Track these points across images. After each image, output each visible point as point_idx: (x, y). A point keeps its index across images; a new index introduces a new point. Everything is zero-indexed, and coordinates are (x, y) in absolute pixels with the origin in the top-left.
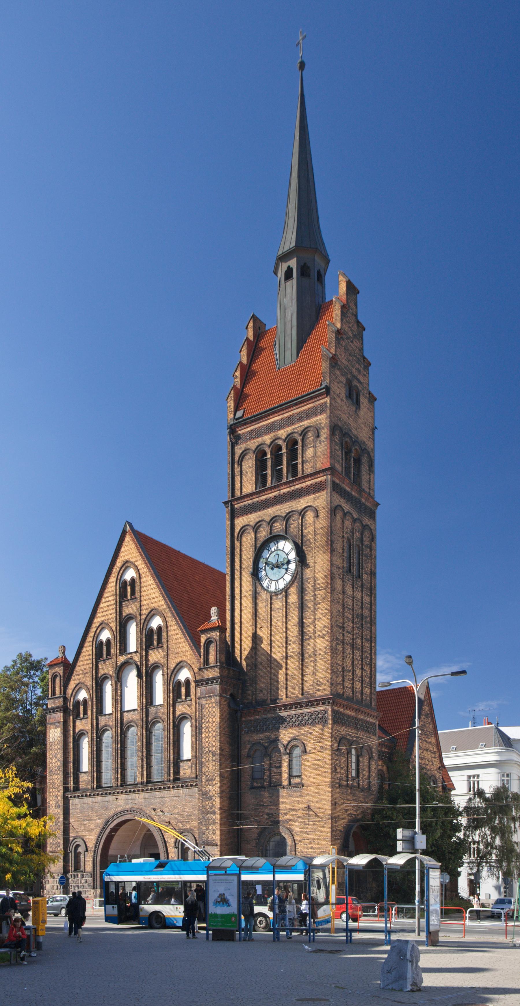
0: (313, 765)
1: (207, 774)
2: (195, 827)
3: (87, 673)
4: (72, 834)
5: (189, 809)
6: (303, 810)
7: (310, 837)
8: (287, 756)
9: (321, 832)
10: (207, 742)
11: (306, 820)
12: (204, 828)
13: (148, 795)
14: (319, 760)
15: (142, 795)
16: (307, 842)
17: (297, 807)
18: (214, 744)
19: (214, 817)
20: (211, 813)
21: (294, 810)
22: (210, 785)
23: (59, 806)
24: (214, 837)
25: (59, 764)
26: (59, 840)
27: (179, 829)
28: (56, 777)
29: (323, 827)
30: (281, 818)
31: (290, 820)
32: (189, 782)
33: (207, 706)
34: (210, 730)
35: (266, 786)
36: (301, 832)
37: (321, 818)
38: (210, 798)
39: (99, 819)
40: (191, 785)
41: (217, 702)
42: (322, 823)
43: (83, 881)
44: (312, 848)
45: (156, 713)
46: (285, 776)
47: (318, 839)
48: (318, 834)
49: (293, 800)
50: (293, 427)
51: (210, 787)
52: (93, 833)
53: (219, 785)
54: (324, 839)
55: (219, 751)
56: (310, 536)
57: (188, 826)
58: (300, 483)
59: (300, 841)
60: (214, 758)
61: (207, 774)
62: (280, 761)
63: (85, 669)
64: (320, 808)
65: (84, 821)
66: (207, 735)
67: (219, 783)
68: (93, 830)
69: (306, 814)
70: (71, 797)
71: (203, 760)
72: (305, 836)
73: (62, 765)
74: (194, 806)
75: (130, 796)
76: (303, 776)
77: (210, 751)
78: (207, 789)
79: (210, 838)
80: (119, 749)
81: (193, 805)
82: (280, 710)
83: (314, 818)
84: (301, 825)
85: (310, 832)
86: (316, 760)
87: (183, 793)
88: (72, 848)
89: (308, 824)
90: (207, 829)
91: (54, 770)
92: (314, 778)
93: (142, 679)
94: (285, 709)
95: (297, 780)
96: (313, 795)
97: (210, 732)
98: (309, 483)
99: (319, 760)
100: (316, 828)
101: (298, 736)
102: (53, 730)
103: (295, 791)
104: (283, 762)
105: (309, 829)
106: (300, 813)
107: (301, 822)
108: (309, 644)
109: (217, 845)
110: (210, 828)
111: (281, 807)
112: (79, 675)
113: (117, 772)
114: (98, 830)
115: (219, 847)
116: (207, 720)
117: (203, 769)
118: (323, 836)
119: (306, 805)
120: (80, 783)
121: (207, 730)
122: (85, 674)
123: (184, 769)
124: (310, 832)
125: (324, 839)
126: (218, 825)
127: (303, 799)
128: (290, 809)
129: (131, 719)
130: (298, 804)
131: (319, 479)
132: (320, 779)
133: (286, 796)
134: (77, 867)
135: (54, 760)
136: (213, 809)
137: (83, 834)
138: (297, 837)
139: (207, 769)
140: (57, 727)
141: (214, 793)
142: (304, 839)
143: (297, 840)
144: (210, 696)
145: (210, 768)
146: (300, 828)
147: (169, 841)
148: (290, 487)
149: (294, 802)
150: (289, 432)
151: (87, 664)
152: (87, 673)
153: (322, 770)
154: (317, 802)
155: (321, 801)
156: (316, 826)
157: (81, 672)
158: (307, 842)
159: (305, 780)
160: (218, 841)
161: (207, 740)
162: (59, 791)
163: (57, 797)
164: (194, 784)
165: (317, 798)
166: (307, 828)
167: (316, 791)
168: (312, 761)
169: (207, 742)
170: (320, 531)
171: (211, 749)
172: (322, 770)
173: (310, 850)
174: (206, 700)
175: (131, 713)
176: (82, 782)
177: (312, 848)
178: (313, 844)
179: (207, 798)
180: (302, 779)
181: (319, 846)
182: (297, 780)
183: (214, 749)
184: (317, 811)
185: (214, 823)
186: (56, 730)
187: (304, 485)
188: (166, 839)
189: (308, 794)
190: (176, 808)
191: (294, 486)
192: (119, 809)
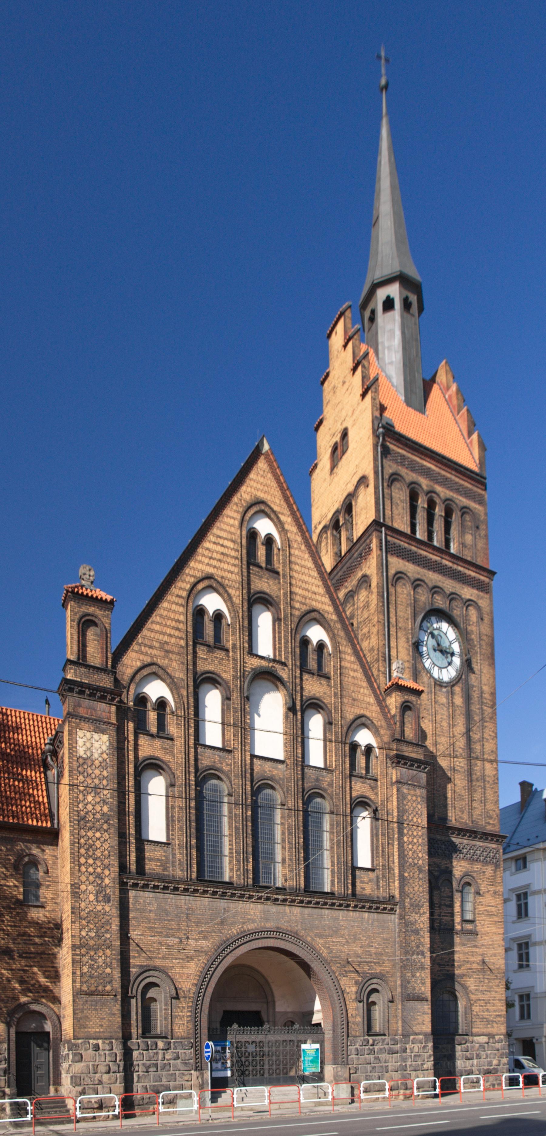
0: (486, 911)
1: (411, 896)
2: (387, 972)
4: (136, 961)
5: (378, 944)
6: (478, 964)
7: (486, 997)
8: (460, 894)
9: (496, 992)
10: (410, 850)
11: (481, 977)
12: (409, 974)
13: (307, 911)
14: (493, 906)
15: (297, 911)
16: (482, 1003)
17: (472, 959)
18: (420, 855)
19: (423, 960)
20: (418, 954)
21: (468, 962)
22: (416, 913)
23: (107, 899)
24: (423, 988)
25: (105, 809)
26: (108, 970)
27: (364, 973)
28: (98, 835)
29: (498, 986)
30: (457, 972)
31: (464, 975)
32: (383, 903)
33: (409, 797)
34: (415, 833)
35: (437, 928)
36: (476, 990)
37: (496, 976)
38: (417, 932)
39: (205, 938)
40: (385, 909)
41: (423, 798)
42: (497, 982)
43: (168, 1056)
44: (488, 1010)
45: (317, 780)
46: (457, 919)
47: (493, 1000)
48: (493, 994)
49: (467, 950)
50: (455, 496)
51: (417, 917)
52: (192, 964)
53: (428, 915)
54: (500, 1000)
55: (427, 868)
56: (473, 636)
57: (378, 970)
58: (464, 567)
59: (475, 1002)
60: (421, 876)
61: (411, 896)
62: (451, 898)
63: (166, 643)
64: (494, 963)
65: (167, 936)
66: (410, 839)
67: (428, 912)
68: (189, 958)
69: (481, 969)
70: (135, 885)
71: (406, 875)
72: (480, 996)
73: (114, 814)
74: (387, 940)
75: (274, 909)
76: (477, 923)
77: (415, 864)
78: (412, 919)
79: (417, 989)
80: (250, 819)
81: (384, 940)
82: (453, 833)
83: (489, 975)
84: (476, 981)
85: (486, 991)
86: (489, 906)
87: (368, 919)
88: (136, 990)
89: (483, 982)
90: (413, 976)
91: (90, 817)
92: (488, 927)
93: (296, 715)
94: (458, 834)
95: (469, 926)
96: (488, 946)
97: (415, 837)
98: (473, 574)
99: (493, 906)
100: (492, 987)
101: (471, 872)
102: (88, 735)
103: (469, 940)
104: (455, 900)
105: (484, 988)
106: (475, 966)
107: (476, 978)
108: (476, 764)
109: (427, 1001)
110: (418, 974)
111: (456, 957)
112: (151, 647)
113: (246, 860)
114: (203, 959)
115: (429, 1003)
116: (410, 818)
117: (406, 888)
118: (498, 996)
119: (480, 958)
120: (147, 862)
121: (410, 833)
122: (167, 651)
123: (362, 882)
124: (486, 991)
125: (500, 1000)
126: (428, 971)
127: (477, 950)
128: (464, 961)
129: (268, 774)
130: (473, 956)
131: (482, 578)
132: (494, 930)
133: (460, 944)
134: (147, 1029)
135: (90, 798)
136: (421, 948)
137: (167, 963)
138: (473, 997)
139: (411, 890)
140: (98, 730)
141: (422, 926)
142: (480, 1000)
143: (472, 1000)
144: (415, 785)
145: (416, 888)
146: (475, 986)
147: (348, 990)
148: (453, 563)
149: (467, 953)
150: (448, 497)
151: (170, 635)
153: (496, 919)
154: (491, 956)
155: (495, 955)
156: (491, 984)
157: (157, 645)
158: (482, 1003)
159: (479, 928)
160: (429, 995)
161: (410, 846)
162: (106, 867)
163: (102, 879)
164: (389, 907)
165: (491, 951)
166: (483, 986)
167: (490, 943)
168: (486, 906)
169: (410, 850)
170: (485, 638)
171: (416, 862)
172: (496, 919)
173: (486, 1013)
174: (409, 789)
175: (269, 763)
176: (151, 860)
177: (488, 1010)
178: (489, 1007)
179: (412, 931)
180: (476, 926)
181: (495, 1008)
182: (469, 926)
183: (420, 862)
184: (492, 967)
185: (422, 968)
186: (96, 736)
187: (468, 572)
188: (342, 987)
189: (483, 945)
190: (359, 939)
191: (458, 565)
192: (251, 927)
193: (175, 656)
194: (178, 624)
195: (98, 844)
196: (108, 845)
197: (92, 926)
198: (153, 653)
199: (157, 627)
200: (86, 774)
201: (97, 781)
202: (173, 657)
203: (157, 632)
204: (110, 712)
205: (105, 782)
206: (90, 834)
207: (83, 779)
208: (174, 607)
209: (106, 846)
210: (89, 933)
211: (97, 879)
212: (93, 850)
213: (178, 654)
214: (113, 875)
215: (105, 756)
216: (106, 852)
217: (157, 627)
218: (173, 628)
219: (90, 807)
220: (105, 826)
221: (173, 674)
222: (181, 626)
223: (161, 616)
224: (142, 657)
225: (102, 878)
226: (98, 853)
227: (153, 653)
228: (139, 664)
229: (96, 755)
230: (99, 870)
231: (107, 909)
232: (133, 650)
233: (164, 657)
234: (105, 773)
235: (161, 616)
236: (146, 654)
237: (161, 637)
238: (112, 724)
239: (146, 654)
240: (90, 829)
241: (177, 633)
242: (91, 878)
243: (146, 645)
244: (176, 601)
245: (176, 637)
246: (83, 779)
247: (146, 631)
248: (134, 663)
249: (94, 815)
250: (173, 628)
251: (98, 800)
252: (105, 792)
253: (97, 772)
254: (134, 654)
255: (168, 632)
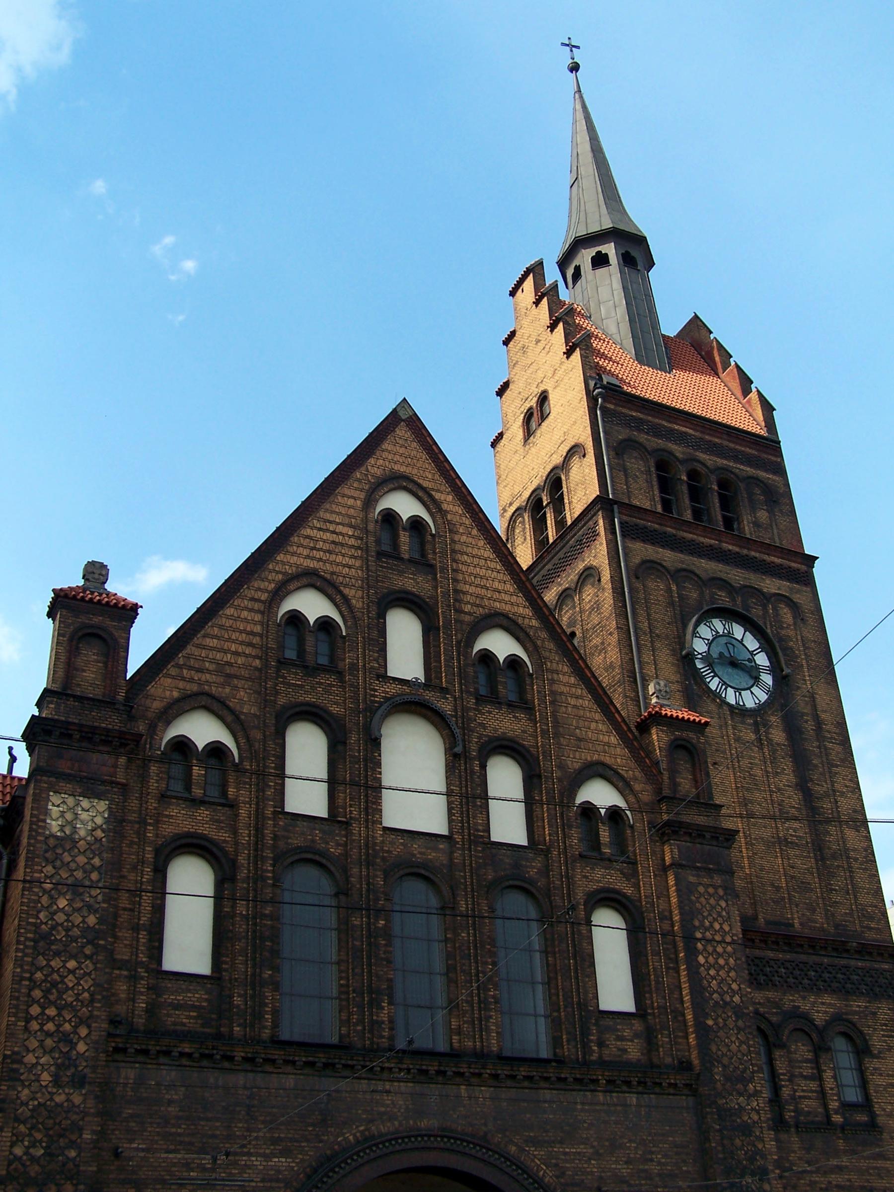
3: (236, 677)
23: (79, 1082)
25: (92, 920)
28: (72, 964)
91: (60, 935)
102: (71, 801)
112: (199, 670)
122: (229, 676)
135: (62, 903)
140: (91, 793)
151: (236, 653)
152: (236, 677)
157: (212, 667)
162: (82, 1022)
186: (85, 803)
193: (243, 682)
194: (251, 637)
195: (70, 981)
196: (91, 982)
197: (38, 1136)
198: (203, 678)
199: (214, 643)
200: (58, 863)
201: (79, 874)
202: (241, 683)
203: (212, 649)
204: (115, 766)
205: (94, 876)
206: (56, 963)
207: (54, 871)
208: (245, 614)
209: (86, 984)
210: (32, 1150)
211: (61, 1045)
212: (58, 992)
213: (249, 679)
214: (95, 1036)
215: (99, 834)
216: (86, 995)
217: (210, 642)
218: (242, 643)
219: (60, 918)
220: (88, 951)
221: (238, 708)
222: (256, 640)
223: (221, 627)
224: (181, 684)
225: (71, 1042)
226: (69, 997)
227: (203, 678)
228: (176, 694)
229: (82, 833)
230: (67, 1027)
231: (77, 1099)
232: (168, 676)
233: (223, 685)
234: (97, 861)
235: (221, 627)
236: (191, 680)
237: (219, 656)
238: (118, 783)
239: (191, 680)
240: (57, 954)
241: (248, 651)
242: (49, 1042)
243: (191, 668)
244: (250, 606)
245: (247, 656)
246: (54, 871)
247: (193, 648)
248: (168, 693)
249: (67, 930)
250: (242, 643)
251: (78, 905)
252: (94, 892)
253: (81, 860)
254: (169, 680)
255: (233, 649)
